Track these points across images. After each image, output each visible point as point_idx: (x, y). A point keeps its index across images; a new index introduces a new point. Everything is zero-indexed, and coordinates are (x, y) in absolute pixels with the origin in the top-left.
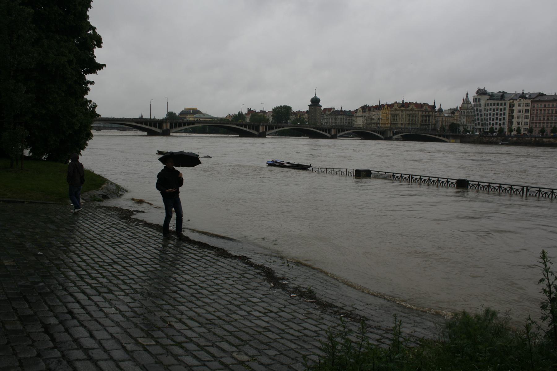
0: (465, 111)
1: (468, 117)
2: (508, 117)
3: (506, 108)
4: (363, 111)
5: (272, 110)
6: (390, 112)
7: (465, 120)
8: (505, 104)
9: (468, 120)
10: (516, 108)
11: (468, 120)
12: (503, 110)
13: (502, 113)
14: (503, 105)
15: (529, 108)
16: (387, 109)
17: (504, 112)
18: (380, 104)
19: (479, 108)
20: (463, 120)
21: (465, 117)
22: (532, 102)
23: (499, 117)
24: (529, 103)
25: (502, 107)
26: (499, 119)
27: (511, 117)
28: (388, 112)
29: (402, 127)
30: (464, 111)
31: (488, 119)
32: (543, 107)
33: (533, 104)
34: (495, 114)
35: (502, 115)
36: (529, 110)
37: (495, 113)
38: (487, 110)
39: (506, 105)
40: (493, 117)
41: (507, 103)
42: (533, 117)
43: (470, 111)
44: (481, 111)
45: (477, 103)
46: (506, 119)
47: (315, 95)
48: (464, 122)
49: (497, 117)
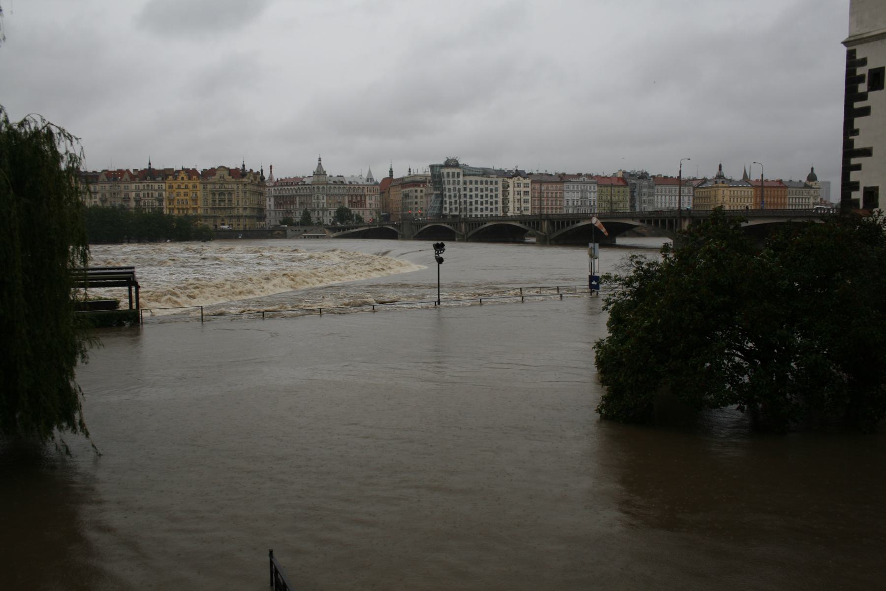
0: (325, 186)
2: (501, 200)
6: (200, 187)
7: (325, 201)
8: (496, 183)
9: (330, 201)
10: (511, 189)
11: (330, 201)
12: (494, 191)
13: (493, 194)
14: (494, 184)
15: (529, 189)
16: (190, 179)
17: (496, 193)
18: (150, 168)
19: (457, 187)
20: (323, 201)
21: (325, 197)
22: (532, 182)
23: (489, 199)
24: (528, 184)
25: (493, 187)
26: (489, 203)
27: (505, 201)
28: (195, 187)
29: (245, 214)
30: (318, 188)
31: (474, 203)
33: (533, 185)
34: (484, 196)
35: (494, 198)
36: (528, 192)
37: (484, 193)
38: (487, 190)
39: (498, 184)
40: (482, 200)
41: (498, 182)
42: (535, 200)
43: (332, 186)
44: (459, 190)
45: (455, 179)
46: (499, 203)
49: (487, 199)
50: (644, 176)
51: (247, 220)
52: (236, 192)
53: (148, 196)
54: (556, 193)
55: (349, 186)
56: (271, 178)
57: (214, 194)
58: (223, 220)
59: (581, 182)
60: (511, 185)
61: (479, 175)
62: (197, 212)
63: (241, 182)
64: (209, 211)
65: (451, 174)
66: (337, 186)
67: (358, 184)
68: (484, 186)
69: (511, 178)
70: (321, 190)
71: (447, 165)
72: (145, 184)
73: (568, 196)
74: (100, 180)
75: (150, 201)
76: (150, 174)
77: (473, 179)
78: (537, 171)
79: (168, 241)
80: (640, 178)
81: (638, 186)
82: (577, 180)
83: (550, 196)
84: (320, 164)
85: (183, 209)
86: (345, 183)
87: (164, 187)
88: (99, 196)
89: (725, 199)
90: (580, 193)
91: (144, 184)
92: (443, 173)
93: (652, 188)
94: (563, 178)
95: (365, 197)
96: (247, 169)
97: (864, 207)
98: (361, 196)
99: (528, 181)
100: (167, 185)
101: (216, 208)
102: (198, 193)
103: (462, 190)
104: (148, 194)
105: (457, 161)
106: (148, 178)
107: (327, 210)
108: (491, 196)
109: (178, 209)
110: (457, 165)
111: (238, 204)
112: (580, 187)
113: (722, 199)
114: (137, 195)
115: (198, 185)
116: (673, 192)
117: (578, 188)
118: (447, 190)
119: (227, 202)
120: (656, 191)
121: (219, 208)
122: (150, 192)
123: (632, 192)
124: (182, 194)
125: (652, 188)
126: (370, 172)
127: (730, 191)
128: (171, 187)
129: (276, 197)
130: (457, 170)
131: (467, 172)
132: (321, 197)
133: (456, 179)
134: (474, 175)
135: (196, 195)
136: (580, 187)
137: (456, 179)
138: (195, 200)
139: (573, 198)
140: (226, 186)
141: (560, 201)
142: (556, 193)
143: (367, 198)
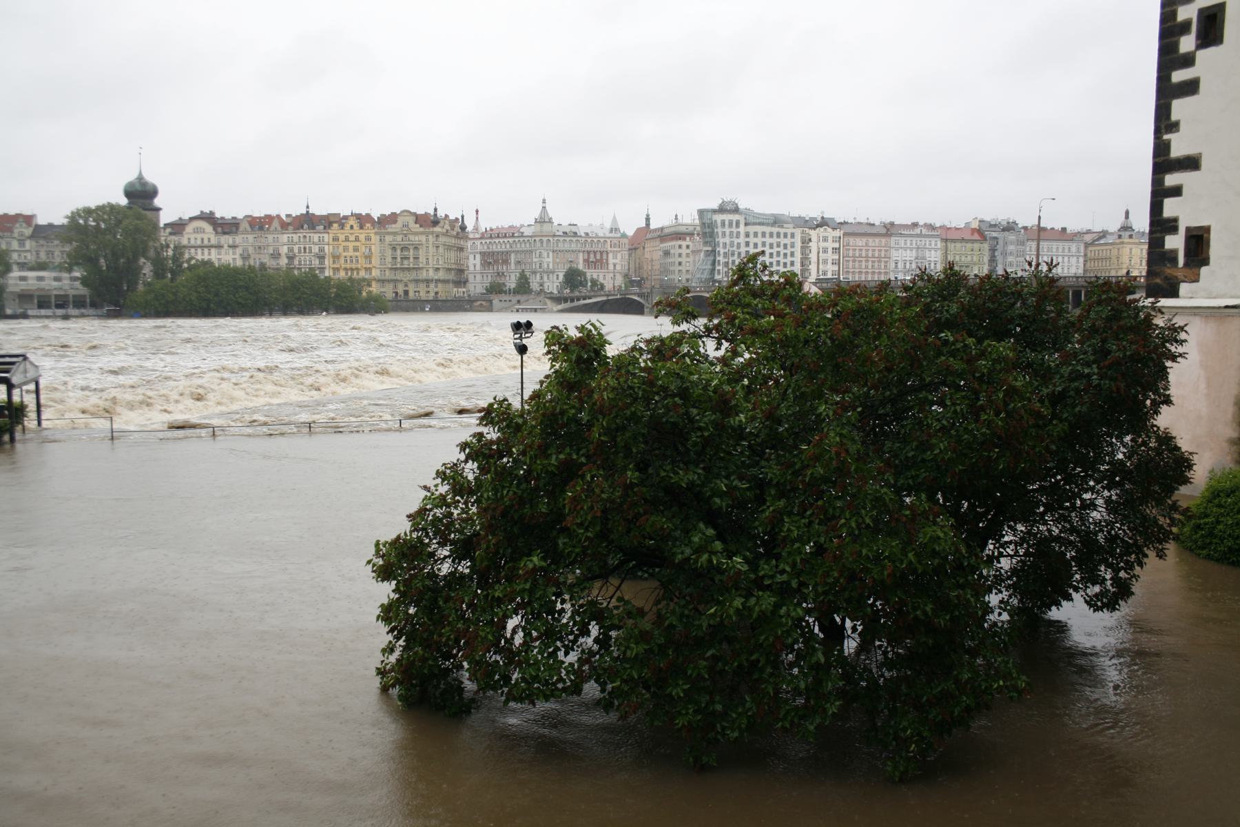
1: (555, 254)
2: (799, 261)
3: (796, 244)
4: (215, 229)
5: (65, 221)
6: (375, 239)
7: (550, 259)
8: (793, 236)
9: (558, 260)
10: (813, 245)
11: (558, 260)
12: (789, 246)
14: (789, 236)
16: (361, 228)
17: (793, 250)
18: (308, 212)
19: (736, 241)
25: (788, 241)
26: (782, 264)
28: (368, 239)
29: (436, 277)
30: (541, 241)
32: (864, 244)
33: (846, 239)
34: (775, 254)
37: (775, 250)
38: (778, 246)
42: (848, 261)
43: (561, 239)
44: (739, 244)
45: (732, 230)
47: (140, 173)
48: (548, 265)
49: (778, 259)
50: (1010, 227)
51: (440, 285)
52: (425, 246)
53: (305, 252)
54: (880, 251)
55: (583, 239)
56: (476, 229)
57: (394, 249)
58: (406, 286)
59: (917, 236)
60: (814, 238)
61: (768, 224)
62: (371, 273)
63: (432, 233)
64: (387, 273)
65: (727, 223)
66: (568, 239)
67: (597, 236)
68: (774, 240)
69: (814, 229)
70: (545, 244)
71: (722, 210)
72: (301, 235)
73: (895, 255)
74: (241, 228)
75: (308, 258)
76: (308, 221)
77: (759, 229)
78: (855, 218)
79: (324, 313)
80: (1004, 230)
81: (1001, 242)
82: (912, 232)
83: (870, 255)
84: (544, 207)
85: (352, 269)
86: (579, 234)
87: (326, 240)
88: (239, 251)
89: (1133, 262)
90: (914, 251)
91: (299, 235)
92: (716, 221)
93: (1023, 244)
94: (890, 230)
95: (607, 253)
96: (441, 214)
97: (1186, 265)
98: (601, 253)
99: (837, 233)
100: (331, 235)
101: (396, 268)
102: (373, 247)
103: (743, 245)
104: (305, 248)
105: (737, 204)
106: (306, 226)
107: (553, 272)
108: (785, 255)
109: (346, 269)
110: (736, 210)
111: (428, 263)
112: (914, 242)
113: (1128, 261)
114: (291, 250)
115: (372, 235)
116: (1054, 250)
117: (911, 244)
118: (721, 245)
119: (411, 260)
120: (1028, 249)
121: (401, 268)
122: (307, 246)
123: (993, 250)
124: (351, 249)
125: (1023, 244)
126: (615, 220)
127: (1142, 250)
128: (336, 239)
129: (483, 254)
130: (735, 217)
131: (751, 220)
132: (545, 254)
133: (734, 230)
134: (760, 224)
135: (370, 250)
136: (914, 242)
137: (734, 230)
138: (368, 257)
139: (904, 258)
140: (412, 238)
141: (886, 262)
142: (880, 251)
143: (611, 255)
